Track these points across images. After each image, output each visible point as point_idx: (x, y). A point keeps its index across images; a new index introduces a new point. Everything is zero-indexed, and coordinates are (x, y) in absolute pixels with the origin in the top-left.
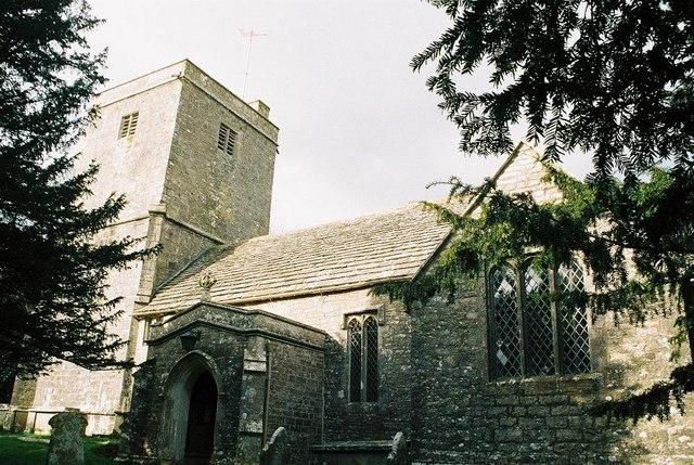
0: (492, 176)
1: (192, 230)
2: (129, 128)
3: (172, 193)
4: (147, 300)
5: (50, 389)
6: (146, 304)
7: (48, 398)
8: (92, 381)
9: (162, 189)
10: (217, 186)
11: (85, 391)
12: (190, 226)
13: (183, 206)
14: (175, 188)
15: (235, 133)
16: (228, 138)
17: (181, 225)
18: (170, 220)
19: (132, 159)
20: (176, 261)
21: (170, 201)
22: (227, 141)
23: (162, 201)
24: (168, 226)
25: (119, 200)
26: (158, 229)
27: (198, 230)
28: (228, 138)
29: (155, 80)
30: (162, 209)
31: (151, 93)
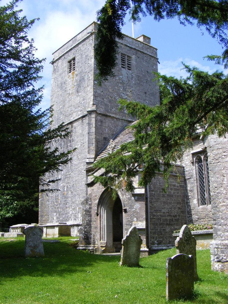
0: (40, 59)
1: (113, 117)
2: (72, 67)
3: (99, 99)
4: (92, 160)
5: (55, 214)
6: (92, 163)
7: (55, 218)
8: (73, 207)
9: (92, 98)
10: (125, 90)
11: (71, 213)
12: (112, 115)
13: (106, 105)
14: (99, 95)
15: (130, 57)
16: (126, 61)
17: (106, 116)
18: (100, 114)
19: (75, 84)
20: (107, 136)
21: (98, 103)
22: (127, 63)
23: (93, 104)
24: (99, 118)
25: (43, 113)
26: (93, 120)
27: (117, 117)
28: (126, 61)
29: (80, 38)
30: (94, 108)
31: (80, 46)
